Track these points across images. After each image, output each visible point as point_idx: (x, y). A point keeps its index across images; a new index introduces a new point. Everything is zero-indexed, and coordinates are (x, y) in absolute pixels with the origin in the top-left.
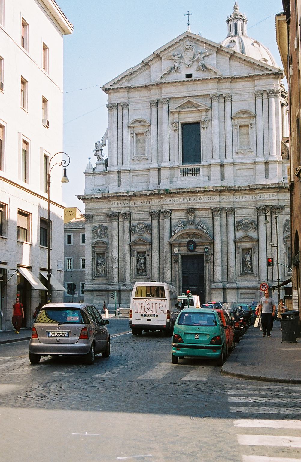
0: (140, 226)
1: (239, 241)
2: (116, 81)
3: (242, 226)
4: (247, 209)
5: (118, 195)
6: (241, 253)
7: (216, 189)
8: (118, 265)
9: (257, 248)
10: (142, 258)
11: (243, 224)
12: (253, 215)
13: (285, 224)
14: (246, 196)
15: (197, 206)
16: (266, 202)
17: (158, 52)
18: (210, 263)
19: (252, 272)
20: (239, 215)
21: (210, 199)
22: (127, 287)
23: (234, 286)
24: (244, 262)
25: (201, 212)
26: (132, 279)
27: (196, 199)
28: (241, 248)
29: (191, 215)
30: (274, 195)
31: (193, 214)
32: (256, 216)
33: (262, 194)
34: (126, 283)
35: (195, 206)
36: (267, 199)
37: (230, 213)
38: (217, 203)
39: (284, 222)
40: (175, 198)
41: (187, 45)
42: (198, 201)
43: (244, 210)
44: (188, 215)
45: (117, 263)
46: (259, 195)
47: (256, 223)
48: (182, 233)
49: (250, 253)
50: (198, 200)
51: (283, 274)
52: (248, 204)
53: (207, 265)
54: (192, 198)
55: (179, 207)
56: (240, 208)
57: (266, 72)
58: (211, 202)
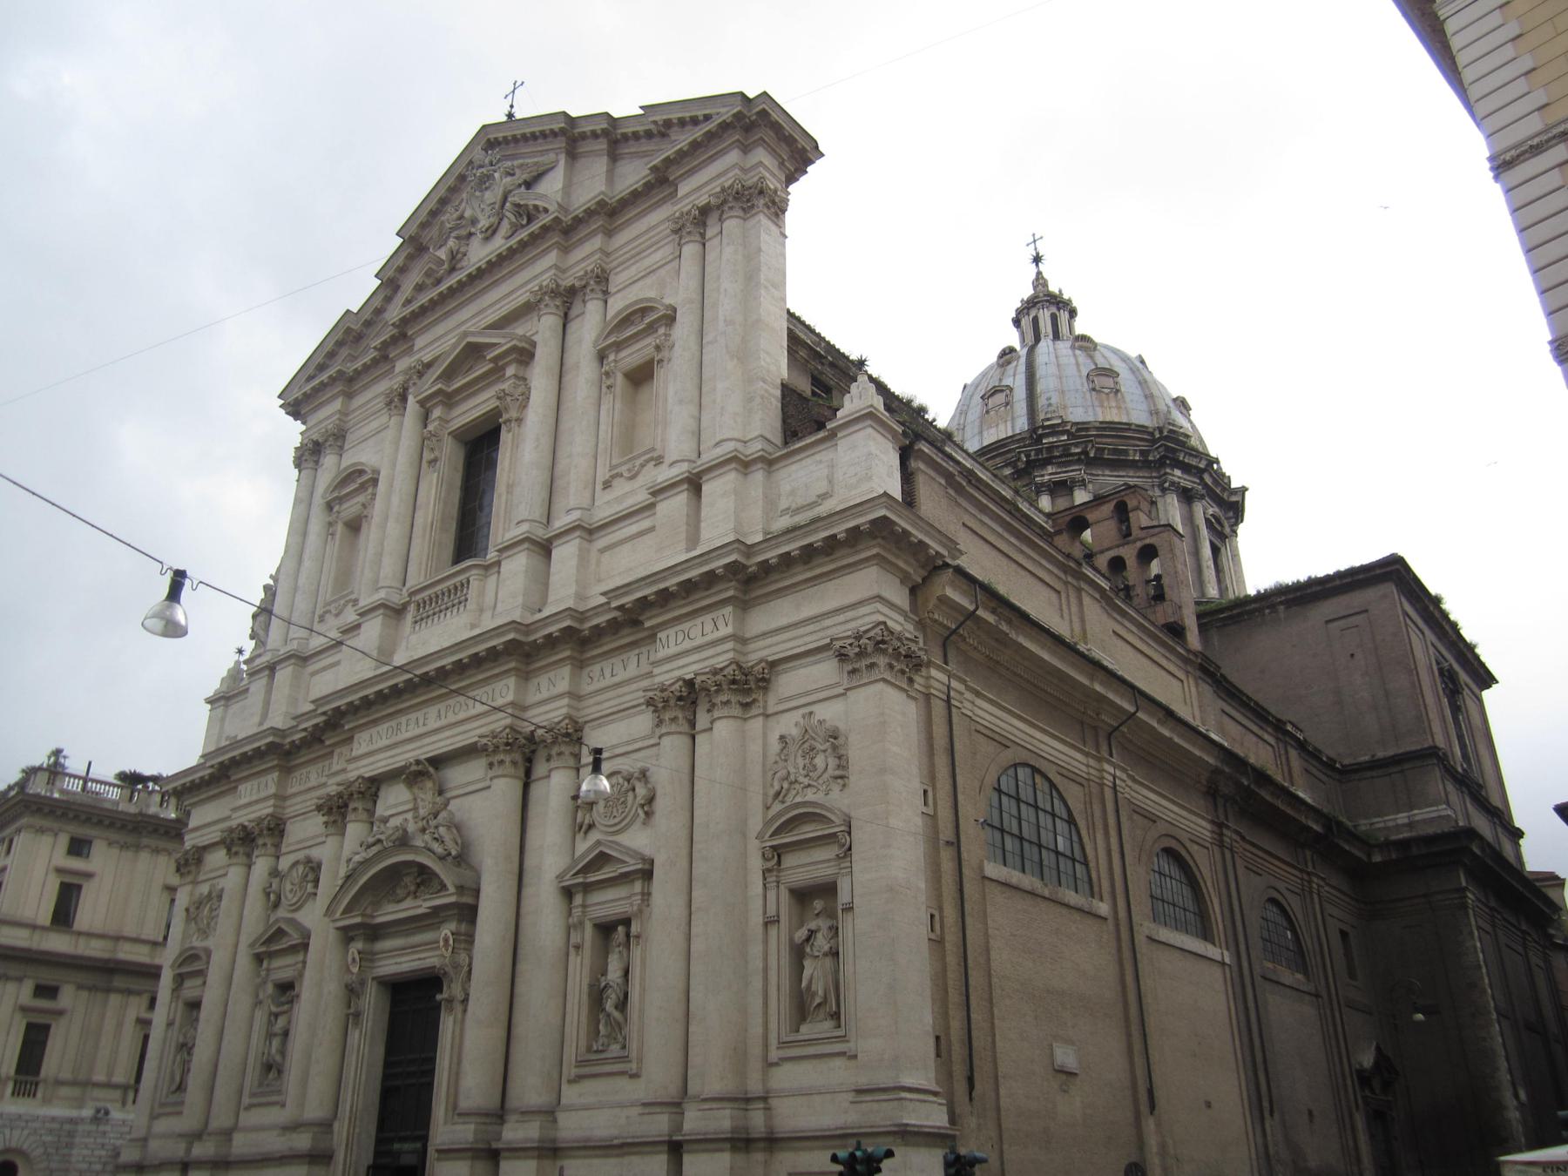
2: (311, 371)
17: (413, 229)
19: (624, 1047)
24: (597, 996)
30: (720, 623)
31: (429, 784)
41: (481, 166)
50: (450, 714)
57: (698, 133)
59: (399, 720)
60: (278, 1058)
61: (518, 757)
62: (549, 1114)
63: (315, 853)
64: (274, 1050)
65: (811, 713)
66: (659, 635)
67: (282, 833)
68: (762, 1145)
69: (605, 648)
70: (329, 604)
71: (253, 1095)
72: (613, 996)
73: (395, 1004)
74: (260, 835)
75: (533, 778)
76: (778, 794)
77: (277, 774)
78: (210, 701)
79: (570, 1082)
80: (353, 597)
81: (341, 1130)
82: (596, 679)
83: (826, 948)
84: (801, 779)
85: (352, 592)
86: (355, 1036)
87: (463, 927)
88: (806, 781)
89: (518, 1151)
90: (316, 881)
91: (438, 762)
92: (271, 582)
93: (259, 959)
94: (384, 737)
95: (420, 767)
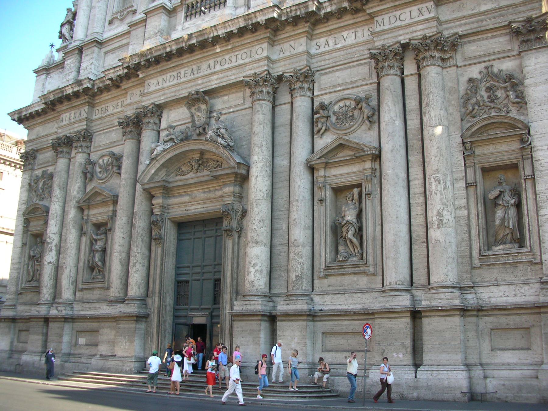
0: (103, 161)
1: (321, 161)
3: (333, 119)
4: (346, 68)
5: (65, 94)
6: (328, 200)
7: (254, 21)
8: (55, 258)
9: (376, 181)
10: (99, 237)
11: (335, 113)
12: (364, 83)
13: (467, 94)
14: (345, 34)
15: (214, 83)
16: (401, 32)
18: (239, 237)
19: (362, 258)
20: (325, 89)
21: (244, 56)
22: (59, 311)
23: (300, 306)
25: (226, 98)
26: (77, 290)
27: (212, 65)
28: (328, 187)
29: (199, 110)
30: (424, 10)
31: (203, 107)
32: (371, 84)
33: (386, 17)
34: (60, 301)
35: (209, 84)
36: (403, 23)
37: (298, 86)
38: (262, 63)
39: (463, 88)
40: (168, 75)
42: (218, 68)
43: (338, 74)
44: (193, 110)
45: (54, 253)
46: (379, 19)
47: (374, 103)
48: (168, 156)
49: (356, 197)
51: (467, 260)
52: (349, 56)
53: (229, 244)
54: (204, 66)
55: (173, 94)
56: (328, 70)
58: (245, 64)
59: (178, 71)
60: (100, 264)
61: (270, 89)
62: (309, 296)
63: (116, 150)
64: (97, 259)
65: (492, 66)
66: (376, 19)
67: (91, 141)
68: (475, 313)
69: (331, 27)
70: (115, 14)
71: (84, 283)
72: (353, 229)
73: (179, 234)
74: (78, 140)
75: (276, 104)
76: (471, 112)
77: (87, 107)
78: (36, 72)
79: (320, 278)
80: (133, 9)
81: (154, 302)
82: (322, 47)
83: (513, 201)
84: (488, 104)
85: (132, 6)
86: (157, 251)
87: (237, 189)
88: (492, 105)
89: (288, 316)
90: (119, 167)
91: (211, 93)
92: (71, 6)
93: (81, 209)
94: (167, 82)
95: (199, 96)
